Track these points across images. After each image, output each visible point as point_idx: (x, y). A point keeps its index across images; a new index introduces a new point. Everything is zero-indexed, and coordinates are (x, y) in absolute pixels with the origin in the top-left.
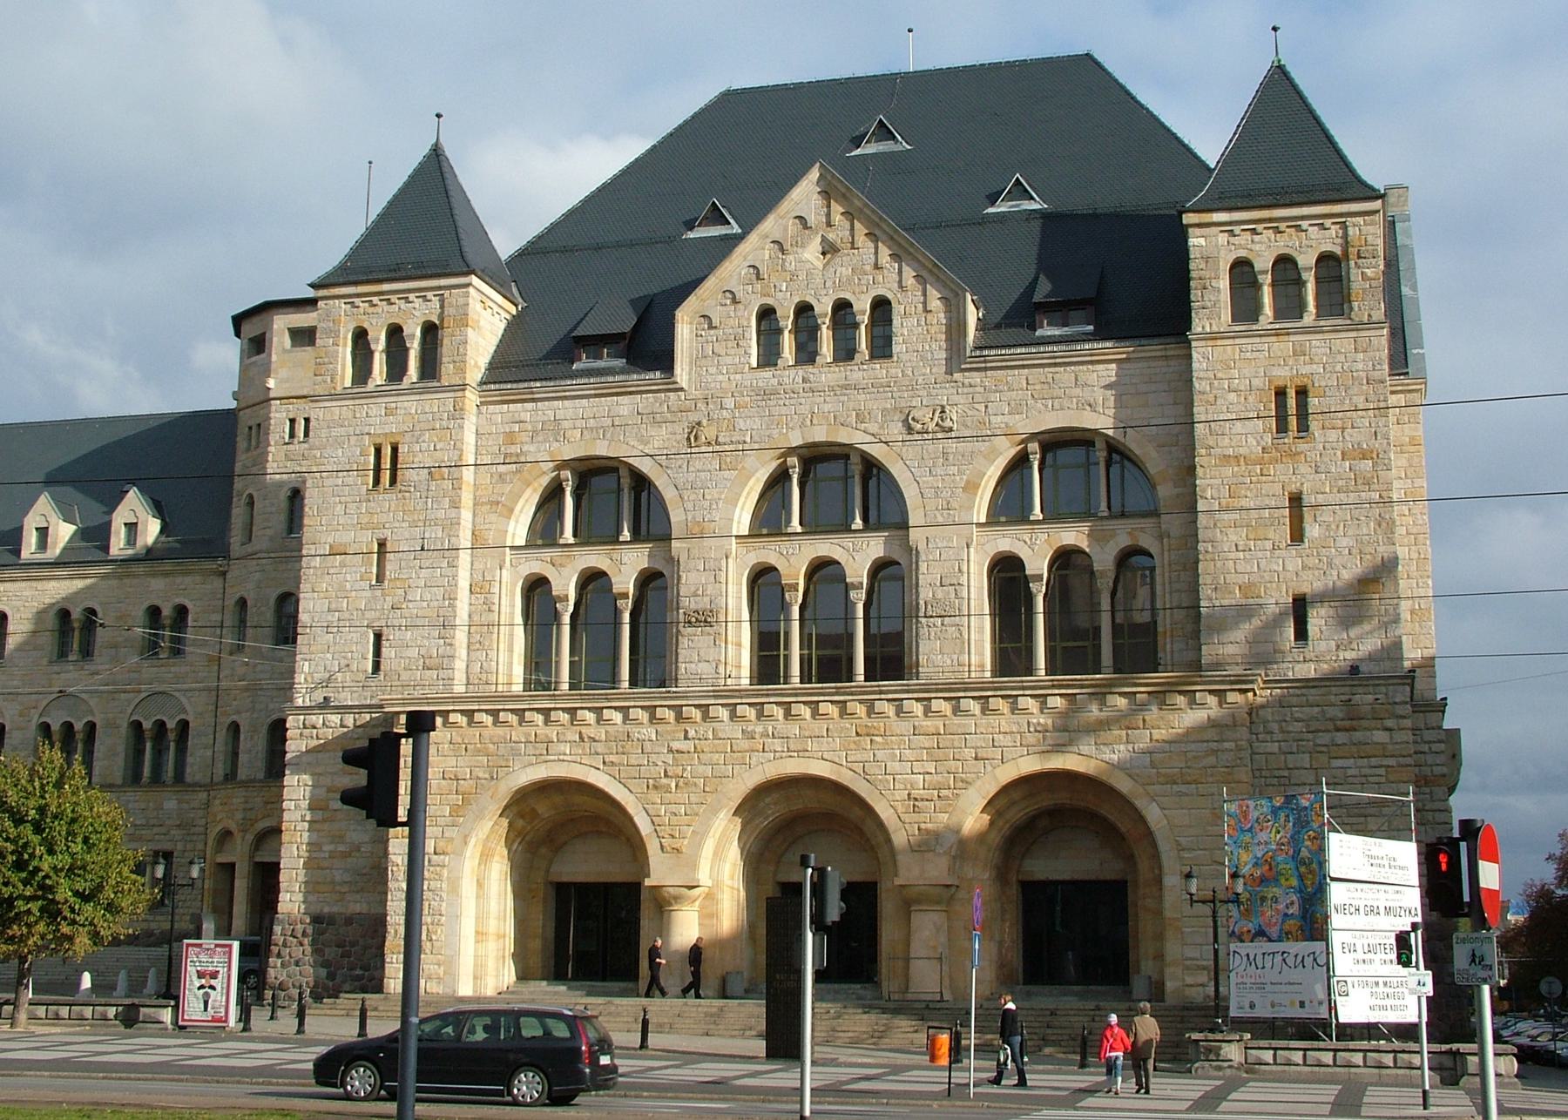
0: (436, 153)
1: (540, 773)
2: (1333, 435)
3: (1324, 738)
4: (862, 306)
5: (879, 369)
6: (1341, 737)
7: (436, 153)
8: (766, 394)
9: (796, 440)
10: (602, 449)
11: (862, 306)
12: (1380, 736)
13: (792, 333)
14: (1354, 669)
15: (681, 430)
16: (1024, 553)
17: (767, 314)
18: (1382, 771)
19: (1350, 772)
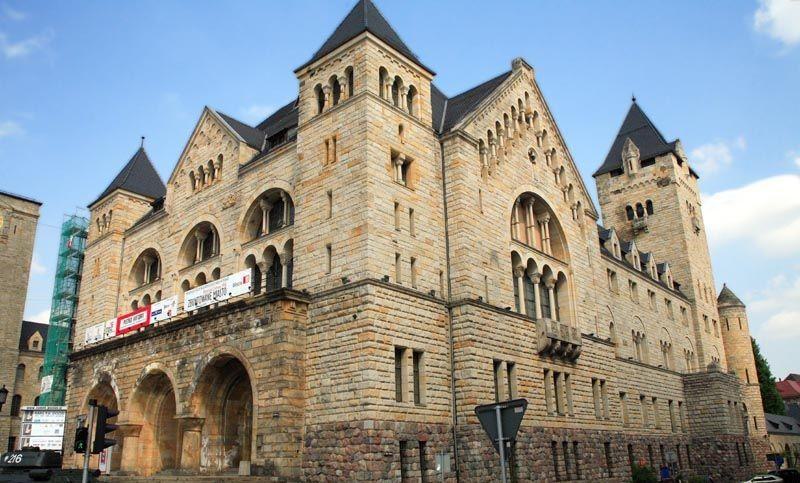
2: (345, 156)
18: (356, 336)
19: (344, 339)
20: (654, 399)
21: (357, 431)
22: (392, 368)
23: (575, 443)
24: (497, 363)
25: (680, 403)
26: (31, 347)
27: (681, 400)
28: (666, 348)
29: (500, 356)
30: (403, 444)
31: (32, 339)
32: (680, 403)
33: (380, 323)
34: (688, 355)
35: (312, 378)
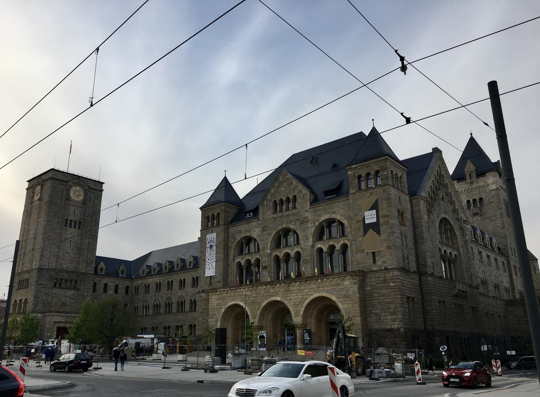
0: (225, 177)
1: (232, 303)
3: (380, 285)
4: (291, 197)
5: (294, 211)
6: (383, 285)
7: (225, 177)
8: (275, 219)
9: (280, 228)
10: (248, 234)
11: (291, 197)
12: (392, 284)
13: (277, 205)
14: (386, 269)
15: (261, 228)
16: (323, 247)
17: (275, 202)
20: (492, 314)
21: (397, 333)
22: (407, 306)
23: (468, 338)
24: (440, 301)
25: (504, 317)
26: (99, 272)
27: (504, 315)
28: (496, 287)
29: (440, 299)
30: (413, 338)
31: (99, 267)
32: (504, 317)
33: (402, 287)
34: (507, 290)
35: (370, 309)
